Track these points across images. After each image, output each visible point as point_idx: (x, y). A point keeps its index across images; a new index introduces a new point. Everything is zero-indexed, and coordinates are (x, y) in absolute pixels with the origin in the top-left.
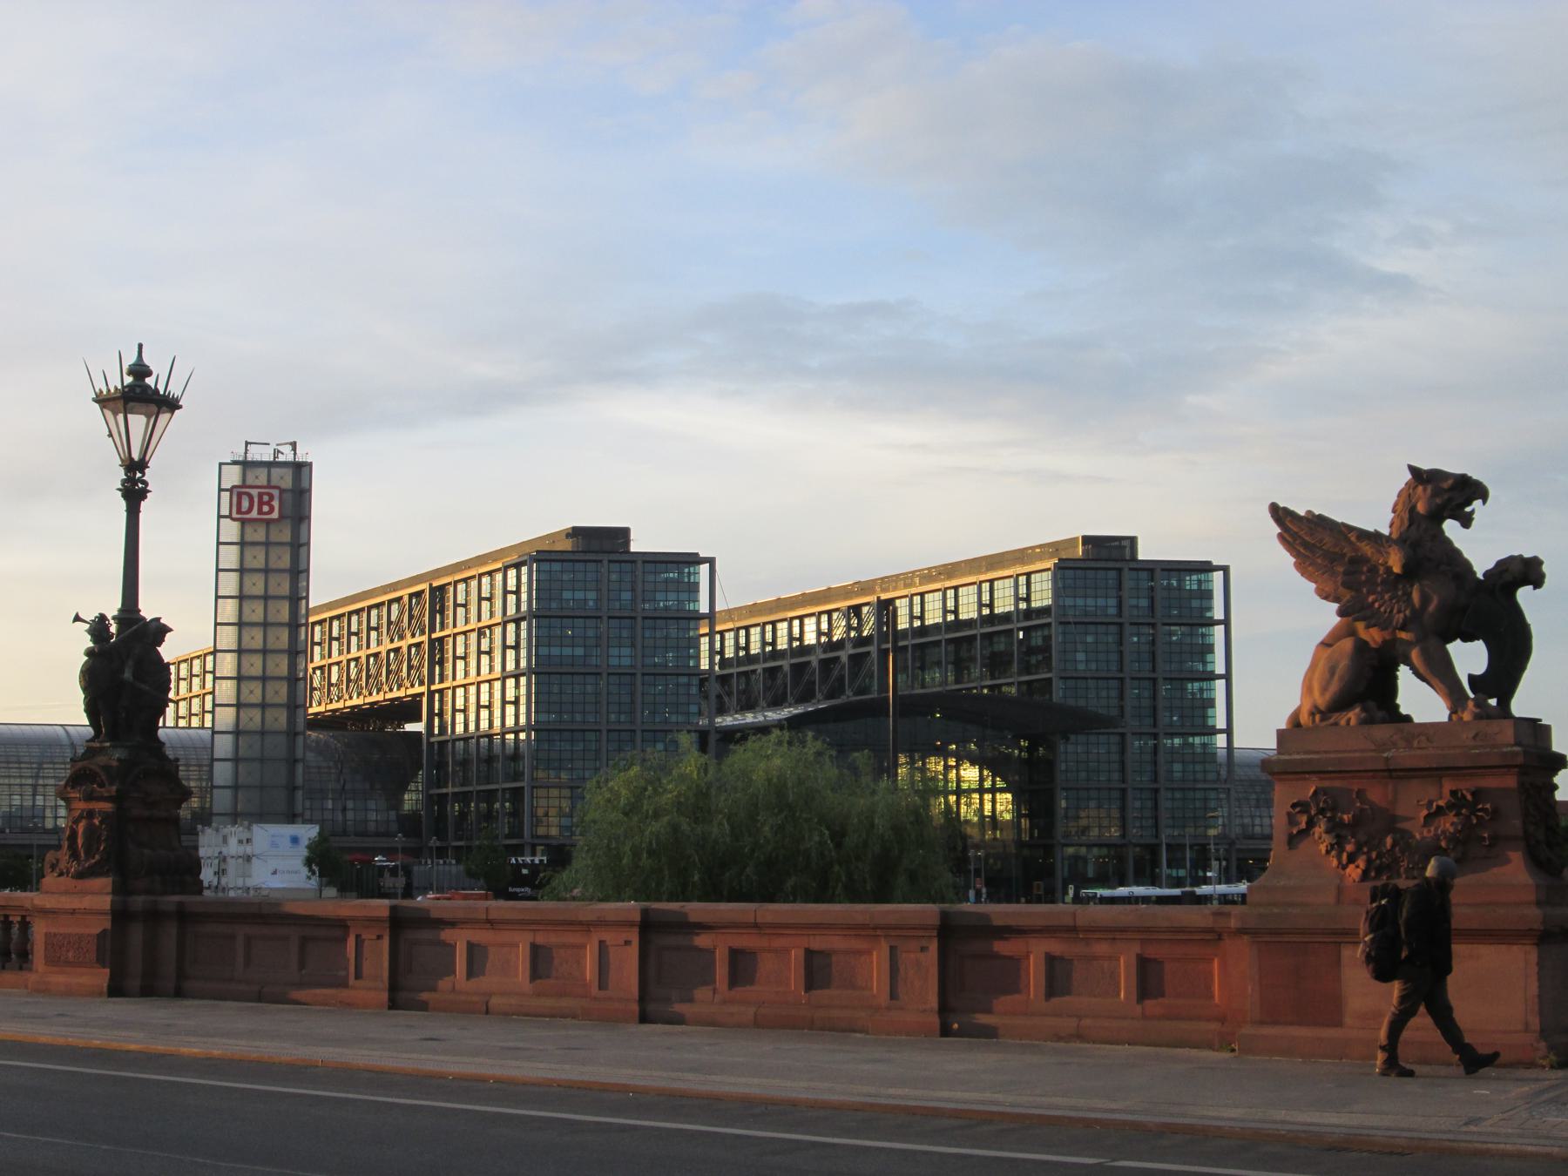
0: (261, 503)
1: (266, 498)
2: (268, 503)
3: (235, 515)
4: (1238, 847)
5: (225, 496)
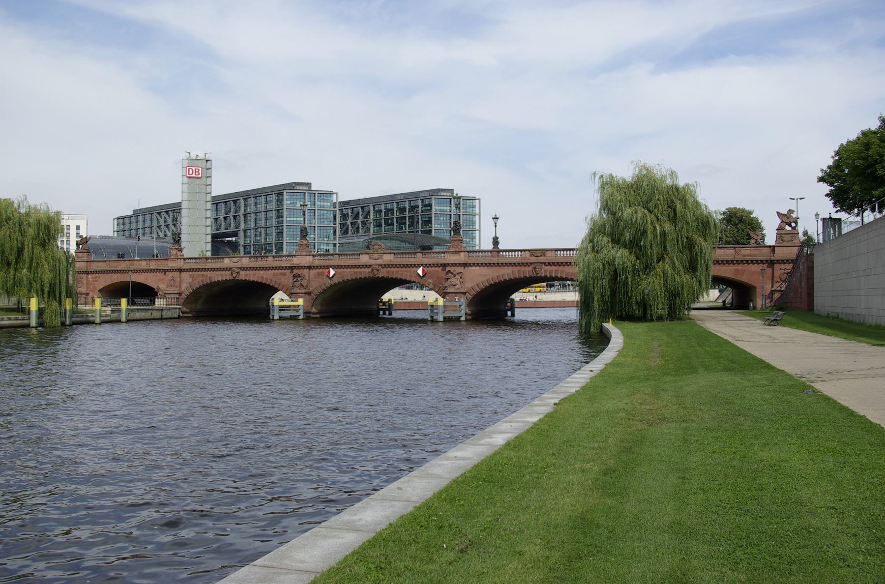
0: (196, 172)
1: (197, 170)
3: (187, 175)
5: (184, 169)
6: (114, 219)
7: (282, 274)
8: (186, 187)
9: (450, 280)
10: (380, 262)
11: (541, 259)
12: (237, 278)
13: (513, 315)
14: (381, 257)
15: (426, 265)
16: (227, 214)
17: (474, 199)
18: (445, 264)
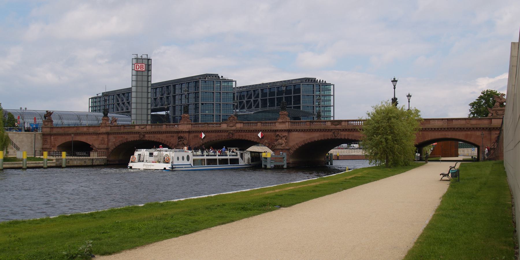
0: (141, 67)
1: (142, 66)
2: (142, 67)
5: (133, 65)
6: (90, 99)
7: (171, 136)
8: (134, 78)
9: (278, 141)
10: (234, 128)
11: (338, 127)
12: (143, 139)
13: (331, 164)
14: (234, 126)
15: (263, 130)
16: (162, 95)
17: (330, 85)
18: (275, 130)
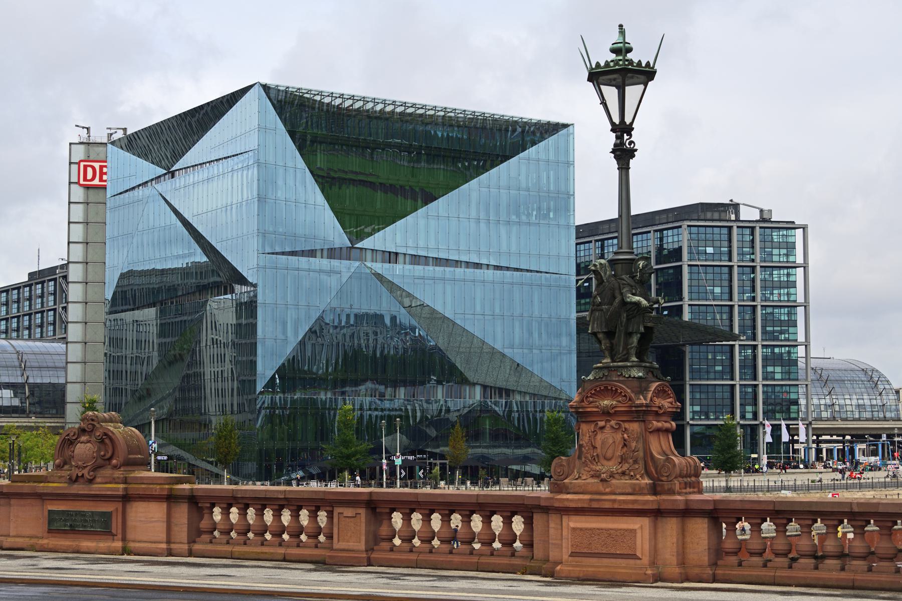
4: (813, 426)
5: (74, 168)
8: (78, 212)
17: (790, 226)
